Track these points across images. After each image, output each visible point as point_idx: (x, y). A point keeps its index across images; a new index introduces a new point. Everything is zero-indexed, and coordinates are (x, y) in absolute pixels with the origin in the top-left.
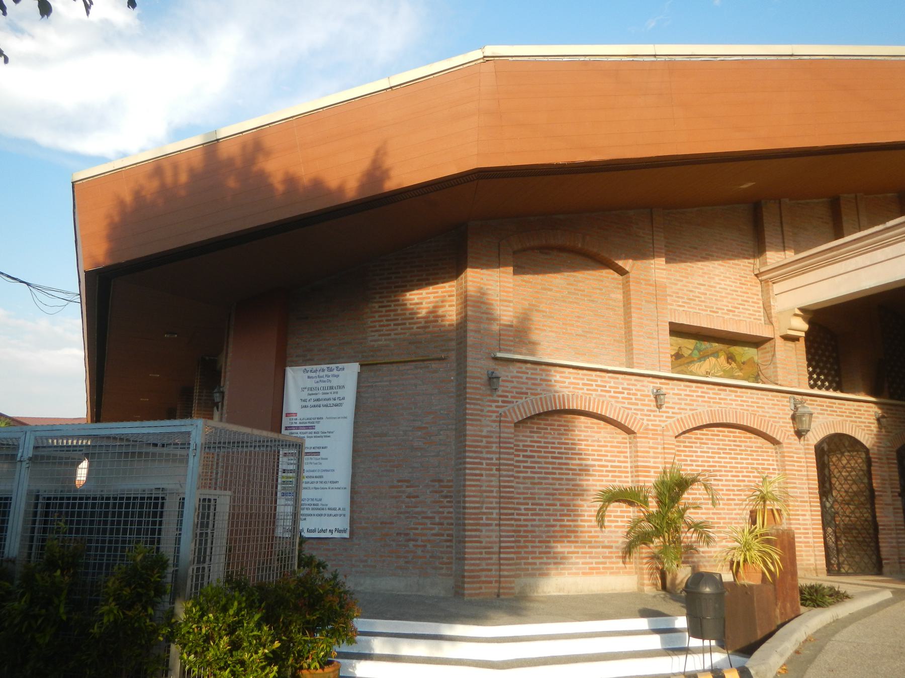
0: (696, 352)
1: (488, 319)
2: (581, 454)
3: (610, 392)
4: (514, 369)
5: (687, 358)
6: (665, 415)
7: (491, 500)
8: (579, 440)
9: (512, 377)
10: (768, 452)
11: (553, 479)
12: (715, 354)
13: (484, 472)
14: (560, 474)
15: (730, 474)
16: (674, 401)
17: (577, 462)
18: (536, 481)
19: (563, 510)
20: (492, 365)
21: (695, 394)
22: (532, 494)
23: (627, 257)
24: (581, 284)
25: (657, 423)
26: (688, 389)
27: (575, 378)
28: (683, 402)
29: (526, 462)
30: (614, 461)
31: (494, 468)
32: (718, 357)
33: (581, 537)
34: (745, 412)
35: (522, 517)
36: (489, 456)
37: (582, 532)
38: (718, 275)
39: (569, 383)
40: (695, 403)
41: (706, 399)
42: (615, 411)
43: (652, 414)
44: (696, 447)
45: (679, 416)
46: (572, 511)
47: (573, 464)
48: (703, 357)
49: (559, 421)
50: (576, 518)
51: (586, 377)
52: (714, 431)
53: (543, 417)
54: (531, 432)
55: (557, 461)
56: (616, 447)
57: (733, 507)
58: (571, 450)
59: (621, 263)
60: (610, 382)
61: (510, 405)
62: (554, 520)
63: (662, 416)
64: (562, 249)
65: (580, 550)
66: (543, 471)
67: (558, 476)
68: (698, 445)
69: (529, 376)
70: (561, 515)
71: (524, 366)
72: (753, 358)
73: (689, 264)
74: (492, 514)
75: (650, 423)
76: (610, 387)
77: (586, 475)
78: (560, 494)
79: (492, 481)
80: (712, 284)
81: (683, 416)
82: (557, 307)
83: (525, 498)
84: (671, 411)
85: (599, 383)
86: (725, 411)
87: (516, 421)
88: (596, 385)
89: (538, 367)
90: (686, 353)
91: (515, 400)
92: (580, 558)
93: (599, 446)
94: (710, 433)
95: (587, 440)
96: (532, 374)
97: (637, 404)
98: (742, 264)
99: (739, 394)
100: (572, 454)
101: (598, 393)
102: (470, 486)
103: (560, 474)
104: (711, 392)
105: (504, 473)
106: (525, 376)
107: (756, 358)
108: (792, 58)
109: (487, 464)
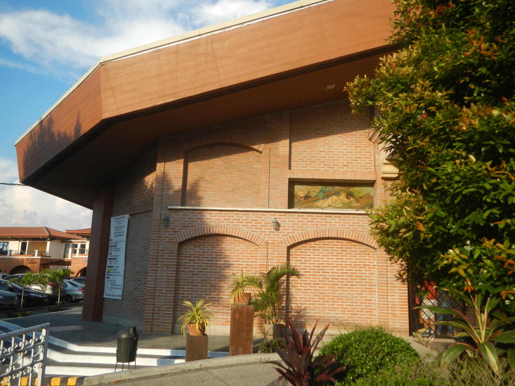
0: (322, 194)
1: (167, 189)
3: (243, 222)
4: (181, 214)
5: (314, 198)
6: (281, 234)
8: (225, 250)
9: (179, 218)
10: (370, 254)
11: (206, 272)
12: (337, 194)
13: (159, 269)
14: (210, 269)
15: (335, 269)
16: (289, 225)
17: (223, 262)
18: (195, 273)
20: (168, 212)
21: (306, 220)
22: (192, 280)
23: (261, 142)
24: (233, 162)
25: (276, 239)
26: (301, 218)
27: (219, 216)
28: (296, 226)
29: (190, 263)
30: (248, 262)
32: (339, 195)
35: (185, 292)
36: (162, 260)
37: (222, 301)
38: (337, 144)
39: (215, 219)
40: (305, 226)
41: (315, 223)
42: (244, 233)
43: (272, 234)
44: (309, 252)
45: (292, 234)
46: (217, 289)
47: (220, 264)
48: (327, 196)
51: (226, 216)
52: (325, 242)
53: (202, 238)
54: (194, 247)
55: (210, 262)
56: (250, 254)
57: (337, 289)
58: (220, 255)
59: (255, 147)
60: (243, 217)
61: (177, 233)
62: (205, 294)
64: (221, 144)
65: (220, 311)
67: (209, 270)
68: (312, 251)
70: (210, 292)
71: (187, 212)
72: (369, 193)
73: (313, 140)
74: (162, 290)
76: (242, 220)
77: (228, 270)
78: (210, 280)
80: (331, 150)
81: (294, 234)
82: (216, 177)
83: (187, 283)
84: (286, 231)
85: (235, 218)
86: (329, 230)
87: (179, 241)
88: (233, 219)
89: (196, 212)
90: (313, 195)
91: (180, 230)
92: (221, 315)
93: (238, 253)
94: (321, 243)
95: (231, 250)
96: (192, 216)
97: (261, 229)
99: (342, 218)
102: (150, 276)
103: (210, 269)
104: (319, 218)
105: (170, 269)
106: (187, 217)
107: (372, 194)
108: (302, 9)
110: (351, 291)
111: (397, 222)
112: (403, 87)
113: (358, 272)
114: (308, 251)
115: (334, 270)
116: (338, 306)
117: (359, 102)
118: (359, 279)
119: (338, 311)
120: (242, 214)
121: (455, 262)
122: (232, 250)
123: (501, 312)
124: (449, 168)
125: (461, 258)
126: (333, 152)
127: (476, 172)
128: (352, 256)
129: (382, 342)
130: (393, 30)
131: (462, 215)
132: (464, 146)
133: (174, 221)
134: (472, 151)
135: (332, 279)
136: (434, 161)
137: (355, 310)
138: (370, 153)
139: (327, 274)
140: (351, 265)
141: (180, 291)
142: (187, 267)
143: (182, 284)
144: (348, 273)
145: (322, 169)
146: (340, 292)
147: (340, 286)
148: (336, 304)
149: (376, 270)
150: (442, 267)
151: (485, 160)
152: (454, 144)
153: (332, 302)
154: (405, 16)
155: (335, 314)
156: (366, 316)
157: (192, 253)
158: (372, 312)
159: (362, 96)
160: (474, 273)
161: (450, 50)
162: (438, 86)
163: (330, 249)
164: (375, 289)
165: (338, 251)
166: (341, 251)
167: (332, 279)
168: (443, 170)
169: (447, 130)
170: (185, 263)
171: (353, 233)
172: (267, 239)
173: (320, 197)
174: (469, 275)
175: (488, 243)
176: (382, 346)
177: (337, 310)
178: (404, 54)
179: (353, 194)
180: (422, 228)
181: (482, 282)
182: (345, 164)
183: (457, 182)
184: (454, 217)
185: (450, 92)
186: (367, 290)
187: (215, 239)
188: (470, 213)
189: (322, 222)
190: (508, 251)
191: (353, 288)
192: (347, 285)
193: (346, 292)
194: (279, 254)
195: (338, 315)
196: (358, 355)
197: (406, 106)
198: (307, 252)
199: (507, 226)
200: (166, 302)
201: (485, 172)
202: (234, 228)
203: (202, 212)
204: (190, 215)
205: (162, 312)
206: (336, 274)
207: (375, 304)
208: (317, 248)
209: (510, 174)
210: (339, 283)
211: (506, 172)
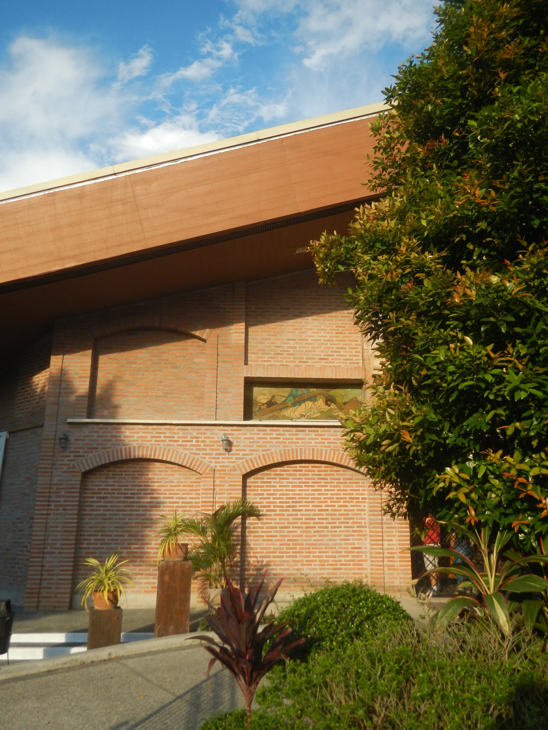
0: (291, 398)
1: (66, 393)
2: (153, 494)
3: (178, 441)
4: (86, 431)
5: (280, 404)
6: (234, 457)
7: (56, 533)
8: (152, 482)
9: (84, 436)
10: (358, 483)
11: (123, 515)
12: (313, 398)
13: (51, 512)
15: (311, 504)
16: (245, 444)
18: (108, 517)
19: (131, 540)
21: (269, 437)
22: (102, 527)
23: (205, 327)
25: (226, 464)
26: (262, 433)
27: (143, 433)
28: (255, 445)
29: (100, 502)
30: (186, 498)
31: (62, 508)
32: (315, 401)
33: (146, 561)
34: (324, 449)
35: (91, 546)
36: (57, 499)
37: (147, 557)
38: (311, 329)
39: (138, 437)
40: (268, 445)
41: (282, 440)
43: (221, 457)
44: (274, 482)
45: (250, 457)
46: (140, 540)
47: (144, 502)
48: (298, 402)
49: (134, 468)
50: (143, 546)
51: (154, 431)
52: (296, 467)
54: (106, 478)
55: (129, 500)
56: (189, 486)
57: (313, 534)
59: (197, 333)
60: (179, 433)
62: (121, 548)
63: (232, 458)
65: (144, 572)
66: (115, 508)
67: (128, 512)
68: (277, 480)
69: (100, 434)
70: (128, 544)
71: (96, 427)
72: (356, 398)
73: (278, 323)
75: (218, 465)
76: (178, 437)
77: (156, 511)
78: (129, 527)
79: (57, 519)
80: (303, 337)
81: (252, 457)
82: (140, 376)
83: (95, 531)
84: (241, 453)
85: (168, 435)
87: (83, 470)
88: (165, 437)
89: (109, 427)
90: (279, 400)
91: (85, 454)
92: (144, 578)
93: (171, 486)
95: (160, 482)
96: (103, 432)
97: (206, 450)
98: (340, 315)
99: (320, 433)
100: (145, 494)
101: (165, 443)
103: (131, 510)
104: (287, 433)
106: (96, 434)
107: (360, 398)
109: (55, 506)
110: (332, 536)
111: (376, 431)
112: (384, 248)
113: (343, 508)
114: (272, 481)
115: (308, 506)
116: (315, 559)
117: (327, 267)
118: (344, 519)
119: (315, 565)
120: (178, 429)
121: (454, 485)
122: (163, 481)
123: (516, 550)
124: (441, 354)
125: (460, 478)
126: (307, 340)
127: (474, 358)
128: (334, 486)
129: (360, 601)
130: (373, 172)
131: (461, 418)
132: (461, 325)
133: (76, 440)
134: (470, 332)
135: (306, 519)
136: (422, 346)
137: (339, 563)
138: (357, 341)
139: (299, 513)
140: (333, 498)
141: (83, 544)
142: (95, 508)
143: (86, 533)
144: (328, 510)
145: (291, 364)
146: (317, 538)
147: (317, 529)
148: (311, 555)
149: (366, 504)
150: (438, 492)
151: (485, 344)
152: (448, 323)
153: (306, 552)
154: (387, 153)
155: (310, 569)
156: (353, 571)
157: (103, 487)
158: (361, 565)
159: (331, 260)
160: (479, 498)
161: (442, 198)
162: (429, 246)
163: (303, 477)
164: (366, 531)
165: (314, 479)
166: (318, 479)
167: (306, 519)
168: (434, 358)
169: (439, 304)
170: (92, 502)
171: (334, 453)
172: (213, 464)
173: (289, 403)
174: (472, 501)
175: (495, 457)
176: (360, 608)
177: (313, 563)
178: (385, 204)
179: (334, 398)
180: (407, 437)
181: (489, 510)
182: (323, 357)
183: (452, 373)
184: (451, 421)
185: (444, 254)
186: (355, 534)
187: (137, 467)
188: (470, 415)
189: (292, 439)
190: (518, 466)
191: (336, 531)
192: (327, 527)
193: (325, 538)
194: (230, 485)
195: (315, 572)
196: (326, 621)
197: (387, 272)
198: (270, 482)
199: (517, 431)
200: (62, 562)
201: (486, 359)
202: (165, 449)
203: (118, 426)
204: (101, 431)
205: (55, 577)
206: (312, 513)
207: (366, 553)
208: (285, 476)
209: (516, 361)
210: (316, 525)
211: (512, 359)
